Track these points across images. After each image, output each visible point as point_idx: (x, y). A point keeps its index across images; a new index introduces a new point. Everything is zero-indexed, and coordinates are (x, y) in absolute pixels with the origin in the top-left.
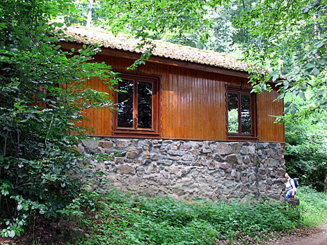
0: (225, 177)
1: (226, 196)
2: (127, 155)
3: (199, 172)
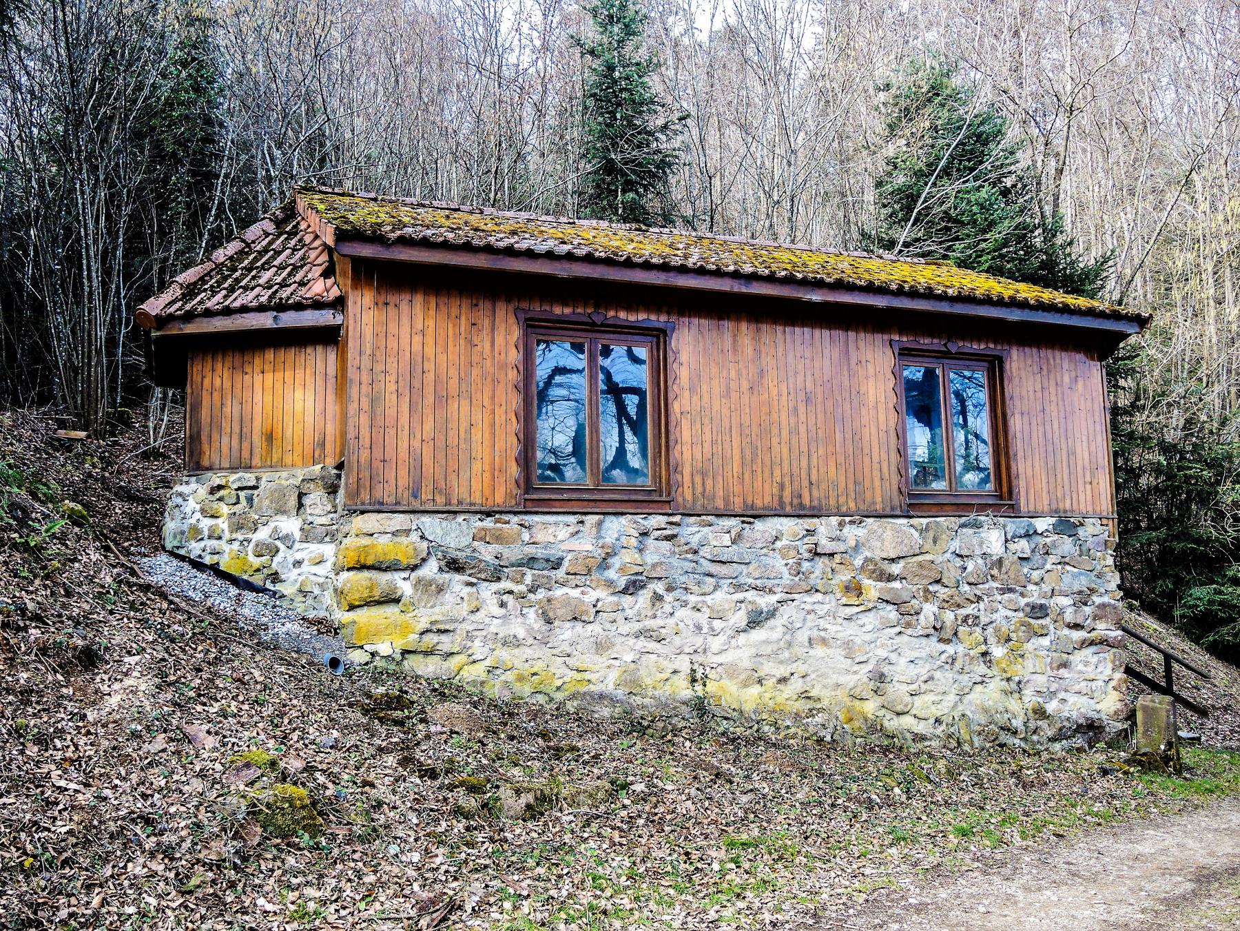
0: (898, 629)
1: (905, 688)
2: (566, 563)
3: (809, 613)
